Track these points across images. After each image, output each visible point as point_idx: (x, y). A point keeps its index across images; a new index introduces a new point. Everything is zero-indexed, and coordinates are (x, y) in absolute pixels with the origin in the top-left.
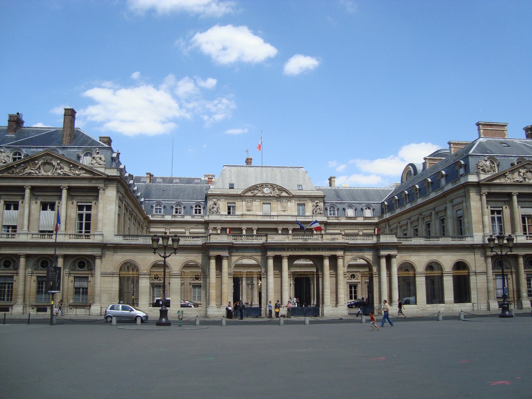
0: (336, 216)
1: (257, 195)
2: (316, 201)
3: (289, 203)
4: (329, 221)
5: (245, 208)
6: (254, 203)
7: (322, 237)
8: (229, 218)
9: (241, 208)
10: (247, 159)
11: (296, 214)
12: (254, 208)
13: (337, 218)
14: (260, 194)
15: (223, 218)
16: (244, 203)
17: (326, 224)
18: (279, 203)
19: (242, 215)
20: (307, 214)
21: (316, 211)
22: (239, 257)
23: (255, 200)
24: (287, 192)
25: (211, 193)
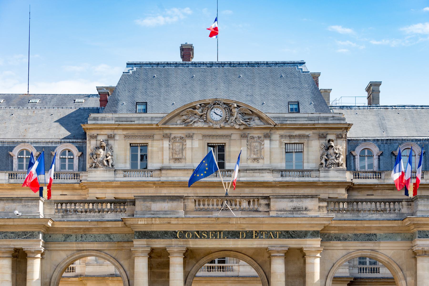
0: (375, 169)
1: (196, 125)
2: (329, 137)
3: (267, 142)
4: (357, 181)
5: (167, 155)
6: (188, 143)
7: (268, 205)
8: (136, 177)
9: (160, 152)
10: (182, 49)
11: (283, 165)
12: (188, 154)
13: (378, 174)
14: (200, 125)
15: (120, 177)
16: (166, 144)
17: (351, 188)
18: (244, 142)
19: (160, 170)
20: (306, 166)
21: (326, 160)
22: (69, 253)
23: (190, 137)
24: (260, 118)
25: (93, 122)
